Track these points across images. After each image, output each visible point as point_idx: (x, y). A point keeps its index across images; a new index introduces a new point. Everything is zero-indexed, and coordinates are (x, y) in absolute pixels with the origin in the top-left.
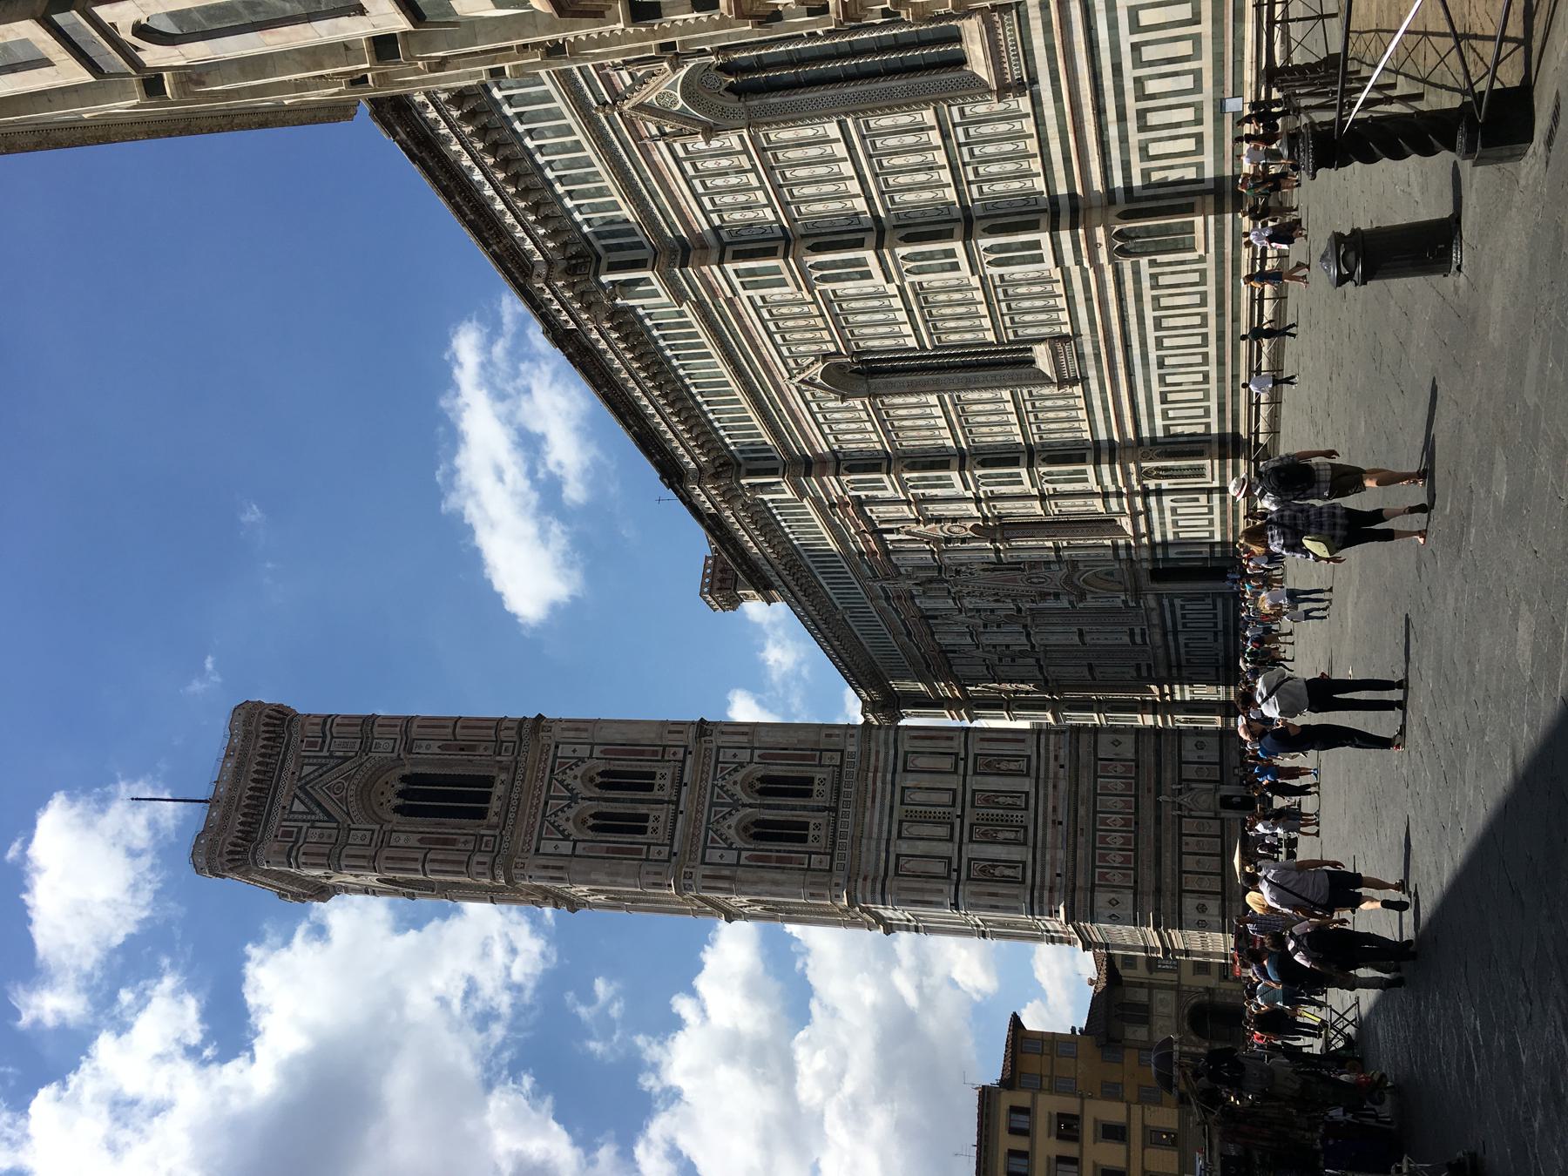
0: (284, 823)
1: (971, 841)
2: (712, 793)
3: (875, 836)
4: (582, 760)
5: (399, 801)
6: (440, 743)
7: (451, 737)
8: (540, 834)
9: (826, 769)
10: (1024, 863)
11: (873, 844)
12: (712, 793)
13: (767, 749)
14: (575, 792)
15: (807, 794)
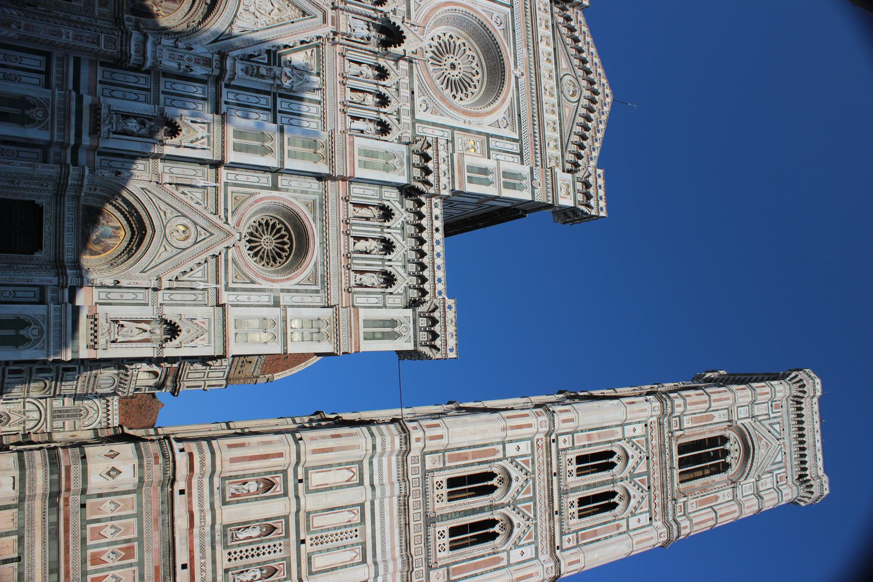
0: (780, 414)
1: (286, 518)
2: (535, 510)
3: (386, 500)
4: (633, 514)
5: (727, 446)
6: (719, 501)
7: (715, 508)
8: (647, 440)
9: (439, 564)
10: (224, 503)
11: (388, 493)
12: (535, 510)
13: (498, 569)
14: (633, 483)
15: (454, 531)
